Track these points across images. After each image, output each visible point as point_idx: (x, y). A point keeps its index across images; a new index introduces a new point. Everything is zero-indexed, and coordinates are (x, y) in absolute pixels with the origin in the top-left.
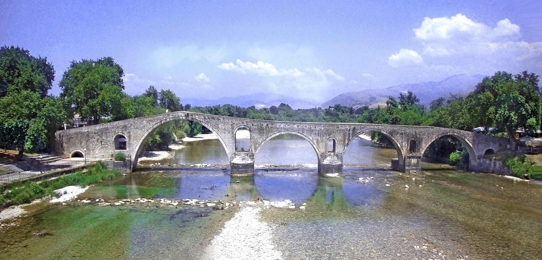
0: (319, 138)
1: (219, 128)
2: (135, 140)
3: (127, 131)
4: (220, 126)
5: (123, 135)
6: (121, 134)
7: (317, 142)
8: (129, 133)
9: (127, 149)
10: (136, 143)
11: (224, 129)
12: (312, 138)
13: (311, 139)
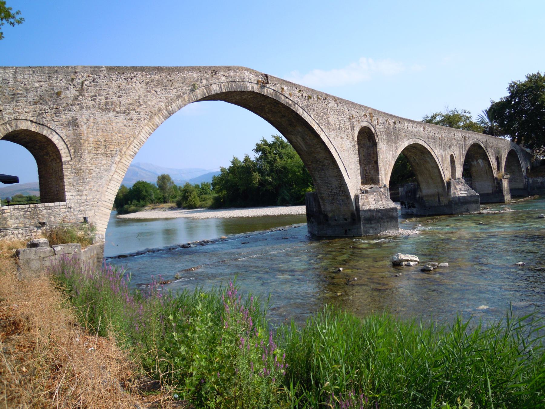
1: (331, 125)
3: (65, 117)
4: (331, 120)
5: (45, 132)
6: (33, 128)
8: (74, 123)
9: (68, 195)
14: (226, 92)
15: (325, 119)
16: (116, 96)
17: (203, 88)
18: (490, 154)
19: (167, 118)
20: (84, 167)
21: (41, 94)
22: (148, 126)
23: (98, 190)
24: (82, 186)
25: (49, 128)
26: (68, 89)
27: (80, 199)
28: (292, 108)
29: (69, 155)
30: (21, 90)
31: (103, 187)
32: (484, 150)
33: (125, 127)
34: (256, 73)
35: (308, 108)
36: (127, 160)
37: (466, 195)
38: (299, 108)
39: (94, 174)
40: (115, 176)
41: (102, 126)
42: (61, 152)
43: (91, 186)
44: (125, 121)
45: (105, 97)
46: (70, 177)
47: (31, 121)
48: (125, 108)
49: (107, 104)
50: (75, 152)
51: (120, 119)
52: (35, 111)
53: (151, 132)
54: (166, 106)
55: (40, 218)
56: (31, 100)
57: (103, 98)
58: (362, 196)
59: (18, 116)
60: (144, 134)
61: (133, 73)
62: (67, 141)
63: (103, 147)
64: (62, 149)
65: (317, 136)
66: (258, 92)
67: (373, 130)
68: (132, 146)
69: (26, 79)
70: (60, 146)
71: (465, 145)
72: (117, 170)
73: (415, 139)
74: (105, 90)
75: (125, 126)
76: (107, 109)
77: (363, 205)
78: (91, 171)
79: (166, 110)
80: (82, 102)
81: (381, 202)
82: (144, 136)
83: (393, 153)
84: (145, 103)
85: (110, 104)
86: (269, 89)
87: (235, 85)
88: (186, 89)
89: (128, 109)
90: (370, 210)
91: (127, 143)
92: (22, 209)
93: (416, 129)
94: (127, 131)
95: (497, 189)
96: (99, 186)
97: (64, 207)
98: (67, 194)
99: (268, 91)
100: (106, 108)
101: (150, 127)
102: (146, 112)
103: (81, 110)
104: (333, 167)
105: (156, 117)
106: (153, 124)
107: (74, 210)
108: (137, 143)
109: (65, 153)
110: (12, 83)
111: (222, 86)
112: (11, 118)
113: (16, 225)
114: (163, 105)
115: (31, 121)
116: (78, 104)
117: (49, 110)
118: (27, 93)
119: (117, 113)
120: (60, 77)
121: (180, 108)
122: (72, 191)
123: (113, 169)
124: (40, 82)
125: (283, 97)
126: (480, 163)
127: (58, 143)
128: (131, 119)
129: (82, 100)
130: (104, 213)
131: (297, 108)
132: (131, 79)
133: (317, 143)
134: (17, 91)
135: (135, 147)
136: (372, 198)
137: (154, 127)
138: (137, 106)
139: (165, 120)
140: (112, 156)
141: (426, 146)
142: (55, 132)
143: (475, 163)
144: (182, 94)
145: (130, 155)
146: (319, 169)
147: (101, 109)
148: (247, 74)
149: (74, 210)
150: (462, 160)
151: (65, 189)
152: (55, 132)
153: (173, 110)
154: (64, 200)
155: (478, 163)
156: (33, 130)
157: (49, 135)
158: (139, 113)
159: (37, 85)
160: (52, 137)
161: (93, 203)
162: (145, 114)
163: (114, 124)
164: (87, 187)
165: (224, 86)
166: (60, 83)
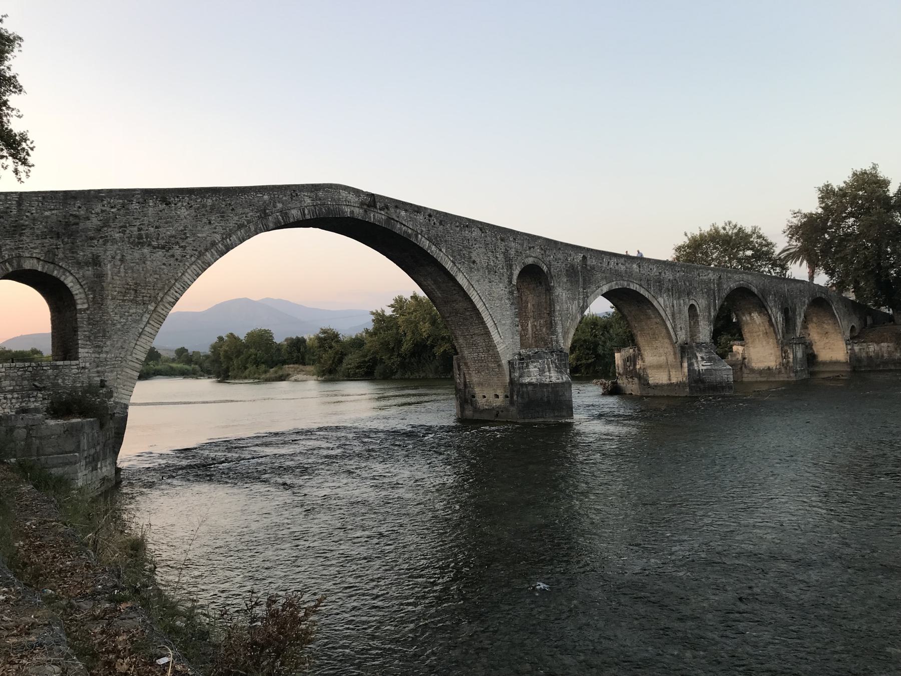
0: (675, 302)
2: (134, 301)
7: (673, 315)
8: (96, 261)
10: (137, 322)
11: (485, 265)
12: (664, 301)
13: (663, 306)
14: (311, 219)
15: (464, 254)
16: (153, 227)
17: (278, 214)
18: (771, 304)
19: (222, 254)
20: (105, 317)
21: (53, 225)
22: (196, 265)
23: (124, 346)
24: (102, 341)
25: (61, 267)
26: (88, 219)
27: (99, 358)
28: (413, 240)
29: (85, 301)
30: (26, 221)
31: (129, 343)
32: (760, 299)
33: (164, 267)
34: (357, 192)
35: (438, 239)
36: (165, 309)
37: (709, 367)
38: (423, 239)
39: (119, 326)
40: (146, 329)
41: (132, 265)
42: (76, 297)
43: (114, 341)
44: (164, 258)
45: (138, 228)
46: (86, 329)
47: (38, 259)
48: (164, 241)
49: (140, 237)
50: (94, 298)
51: (157, 255)
52: (44, 247)
53: (200, 272)
54: (223, 239)
55: (43, 379)
56: (39, 232)
57: (136, 229)
58: (519, 363)
59: (21, 253)
60: (190, 275)
61: (178, 197)
62: (84, 284)
63: (133, 292)
64: (77, 294)
65: (453, 279)
66: (360, 218)
67: (545, 268)
68: (172, 291)
69: (33, 207)
70: (75, 289)
71: (719, 290)
72: (151, 322)
73: (621, 282)
74: (138, 219)
75: (164, 264)
76: (139, 243)
77: (520, 377)
78: (115, 322)
79: (222, 244)
80: (107, 234)
81: (547, 374)
82: (189, 277)
83: (578, 302)
84: (194, 235)
85: (144, 237)
86: (377, 215)
87: (326, 210)
88: (251, 216)
89: (169, 243)
90: (530, 384)
91: (166, 287)
92: (21, 368)
93: (623, 268)
94: (166, 271)
95: (783, 360)
96: (125, 341)
97: (76, 367)
98: (80, 350)
99: (376, 217)
100: (139, 242)
101: (199, 265)
102: (194, 247)
103: (104, 245)
104: (477, 322)
105: (207, 253)
106: (203, 263)
107: (89, 371)
108: (179, 286)
109: (81, 299)
110: (15, 212)
111: (306, 212)
112: (12, 255)
113: (12, 388)
114: (218, 237)
115: (38, 259)
116: (101, 238)
117: (62, 246)
118: (34, 224)
119: (154, 248)
120: (78, 204)
121: (242, 240)
122: (88, 347)
123: (145, 319)
124: (51, 210)
125: (398, 226)
126: (755, 317)
127: (72, 287)
128: (173, 256)
129: (107, 232)
130: (129, 375)
131: (421, 240)
132: (175, 204)
133: (453, 288)
134: (21, 222)
135: (176, 292)
136: (535, 367)
137: (204, 266)
138: (181, 238)
139: (221, 257)
140: (144, 304)
141: (642, 291)
142: (69, 272)
143: (748, 318)
144: (246, 223)
145: (169, 303)
146: (460, 323)
147: (132, 243)
148: (344, 194)
149: (89, 371)
150: (712, 314)
151: (78, 344)
152: (69, 272)
153: (232, 244)
154: (77, 358)
155: (752, 319)
156: (39, 270)
157: (61, 276)
158: (184, 248)
159: (47, 213)
160: (65, 279)
161: (116, 362)
162: (193, 250)
163: (148, 263)
164: (108, 343)
165: (309, 212)
166: (78, 211)
